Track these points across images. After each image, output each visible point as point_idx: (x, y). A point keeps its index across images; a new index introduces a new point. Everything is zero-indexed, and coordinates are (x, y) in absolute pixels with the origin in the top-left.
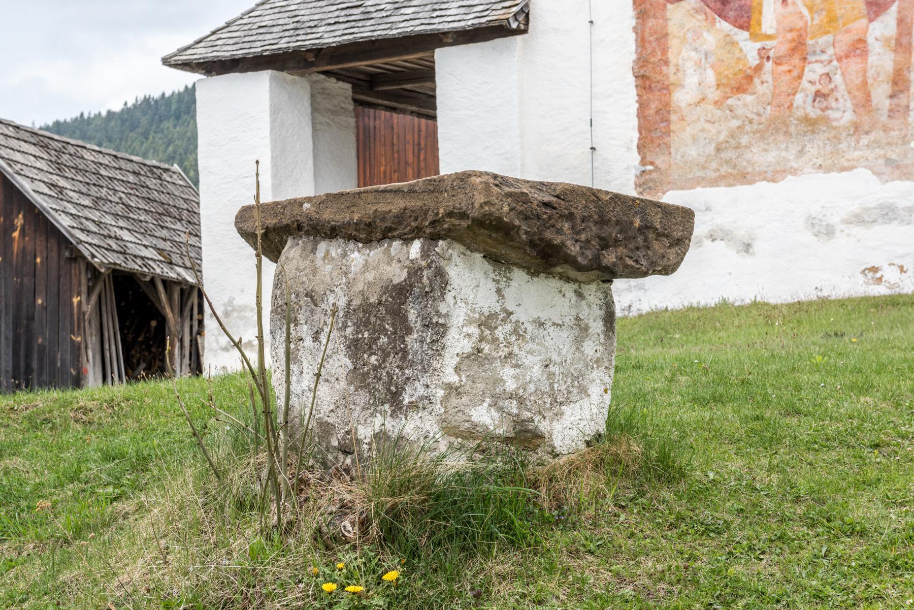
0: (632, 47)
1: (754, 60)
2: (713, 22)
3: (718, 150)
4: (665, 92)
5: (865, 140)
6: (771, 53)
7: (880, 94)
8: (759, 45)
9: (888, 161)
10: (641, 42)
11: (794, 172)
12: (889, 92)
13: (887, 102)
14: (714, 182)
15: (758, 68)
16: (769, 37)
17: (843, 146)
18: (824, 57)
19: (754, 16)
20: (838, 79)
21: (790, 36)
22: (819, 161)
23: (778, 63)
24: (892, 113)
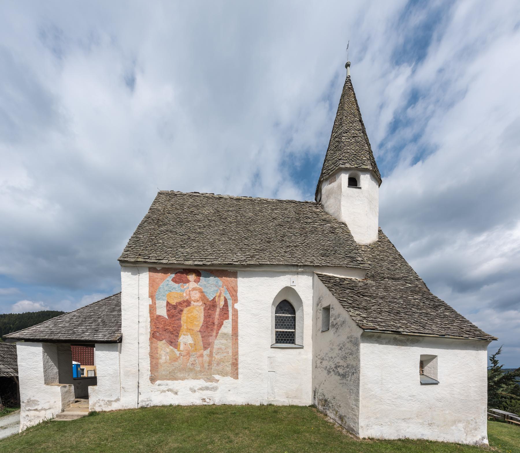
1: (178, 355)
3: (170, 373)
5: (202, 374)
7: (206, 365)
9: (207, 378)
10: (151, 348)
11: (187, 379)
15: (179, 357)
20: (197, 361)
23: (184, 356)
24: (208, 369)
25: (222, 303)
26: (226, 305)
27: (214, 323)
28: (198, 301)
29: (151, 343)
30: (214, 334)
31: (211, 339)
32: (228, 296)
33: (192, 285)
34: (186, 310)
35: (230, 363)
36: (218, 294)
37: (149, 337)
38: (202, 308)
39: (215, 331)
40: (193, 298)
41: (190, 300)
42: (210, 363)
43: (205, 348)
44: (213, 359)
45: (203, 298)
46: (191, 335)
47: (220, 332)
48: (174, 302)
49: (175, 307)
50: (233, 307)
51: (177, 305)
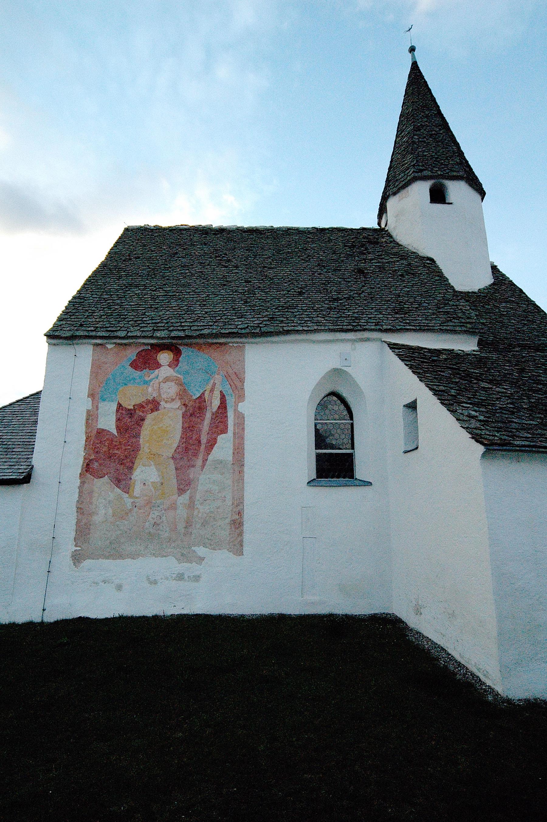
0: (77, 496)
1: (129, 505)
2: (114, 488)
4: (89, 515)
6: (137, 505)
7: (181, 527)
8: (132, 500)
9: (183, 555)
12: (184, 526)
13: (183, 530)
14: (107, 558)
15: (131, 510)
16: (137, 498)
17: (164, 546)
18: (159, 508)
19: (131, 488)
21: (145, 498)
22: (154, 552)
24: (185, 535)
25: (216, 403)
26: (223, 405)
27: (200, 442)
28: (173, 400)
29: (83, 483)
30: (199, 462)
31: (192, 473)
32: (228, 391)
33: (165, 371)
34: (150, 418)
35: (228, 521)
36: (209, 387)
37: (79, 471)
38: (180, 413)
39: (201, 456)
40: (164, 396)
41: (157, 399)
42: (188, 524)
43: (181, 491)
44: (196, 512)
45: (183, 393)
46: (155, 465)
47: (210, 457)
48: (129, 404)
49: (131, 413)
50: (236, 410)
51: (135, 410)
